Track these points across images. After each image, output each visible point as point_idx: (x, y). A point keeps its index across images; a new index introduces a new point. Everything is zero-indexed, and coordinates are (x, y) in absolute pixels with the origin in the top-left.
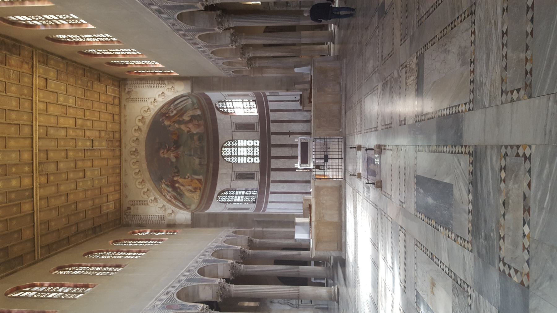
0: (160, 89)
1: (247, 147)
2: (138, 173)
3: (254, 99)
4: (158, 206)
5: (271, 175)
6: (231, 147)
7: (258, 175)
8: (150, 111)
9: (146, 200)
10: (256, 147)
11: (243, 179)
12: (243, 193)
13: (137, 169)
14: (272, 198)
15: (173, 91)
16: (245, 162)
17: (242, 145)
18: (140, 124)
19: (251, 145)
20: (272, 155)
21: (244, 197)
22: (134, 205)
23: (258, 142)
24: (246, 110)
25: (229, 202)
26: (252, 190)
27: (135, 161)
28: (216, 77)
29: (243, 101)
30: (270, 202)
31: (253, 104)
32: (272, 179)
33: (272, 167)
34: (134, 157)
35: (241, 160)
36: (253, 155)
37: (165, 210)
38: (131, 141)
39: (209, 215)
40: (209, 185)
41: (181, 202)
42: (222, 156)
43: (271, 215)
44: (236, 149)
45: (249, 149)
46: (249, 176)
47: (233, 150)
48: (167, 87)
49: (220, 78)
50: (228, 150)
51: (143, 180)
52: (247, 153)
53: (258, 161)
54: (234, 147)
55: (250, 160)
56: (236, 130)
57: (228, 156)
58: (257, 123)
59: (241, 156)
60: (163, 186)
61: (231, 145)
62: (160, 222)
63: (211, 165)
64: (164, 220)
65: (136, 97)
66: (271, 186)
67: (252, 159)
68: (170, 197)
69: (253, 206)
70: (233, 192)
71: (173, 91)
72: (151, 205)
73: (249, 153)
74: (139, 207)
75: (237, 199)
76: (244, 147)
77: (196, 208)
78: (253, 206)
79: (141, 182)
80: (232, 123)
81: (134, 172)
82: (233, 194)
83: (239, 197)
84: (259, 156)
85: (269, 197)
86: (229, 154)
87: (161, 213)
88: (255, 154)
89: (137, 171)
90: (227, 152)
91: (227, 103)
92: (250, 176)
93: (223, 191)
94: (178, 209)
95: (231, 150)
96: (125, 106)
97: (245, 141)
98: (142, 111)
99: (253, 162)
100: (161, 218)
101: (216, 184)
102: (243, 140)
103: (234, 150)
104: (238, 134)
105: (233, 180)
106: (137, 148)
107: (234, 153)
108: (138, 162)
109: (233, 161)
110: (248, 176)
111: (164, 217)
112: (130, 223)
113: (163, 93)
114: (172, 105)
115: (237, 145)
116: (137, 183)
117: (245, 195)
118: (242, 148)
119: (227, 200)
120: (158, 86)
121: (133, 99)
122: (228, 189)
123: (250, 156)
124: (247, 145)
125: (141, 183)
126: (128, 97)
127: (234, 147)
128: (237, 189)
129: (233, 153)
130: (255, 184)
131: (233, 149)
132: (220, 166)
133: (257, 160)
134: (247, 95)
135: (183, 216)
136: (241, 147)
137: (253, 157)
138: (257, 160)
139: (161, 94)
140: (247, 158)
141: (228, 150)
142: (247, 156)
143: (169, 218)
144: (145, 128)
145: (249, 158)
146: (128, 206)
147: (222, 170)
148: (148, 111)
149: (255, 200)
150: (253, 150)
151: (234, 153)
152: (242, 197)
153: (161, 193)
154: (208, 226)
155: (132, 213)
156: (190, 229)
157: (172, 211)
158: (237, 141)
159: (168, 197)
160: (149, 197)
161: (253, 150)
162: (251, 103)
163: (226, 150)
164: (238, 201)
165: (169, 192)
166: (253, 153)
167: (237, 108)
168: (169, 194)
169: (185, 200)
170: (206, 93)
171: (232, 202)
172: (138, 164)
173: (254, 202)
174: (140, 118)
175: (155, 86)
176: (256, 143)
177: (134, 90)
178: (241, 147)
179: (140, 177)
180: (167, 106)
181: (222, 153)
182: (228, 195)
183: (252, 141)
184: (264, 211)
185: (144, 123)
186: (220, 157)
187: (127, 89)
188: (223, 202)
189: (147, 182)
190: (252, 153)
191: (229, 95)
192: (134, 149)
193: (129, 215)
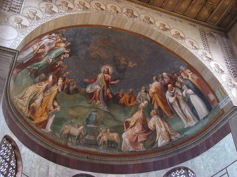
2: (100, 7)
4: (38, 11)
27: (119, 9)
37: (29, 18)
51: (87, 8)
62: (7, 4)
63: (65, 153)
64: (8, 11)
68: (43, 47)
89: (103, 7)
94: (27, 34)
100: (15, 9)
101: (33, 150)
106: (138, 19)
111: (15, 12)
114: (190, 91)
120: (230, 68)
121: (205, 36)
122: (20, 169)
139: (220, 68)
143: (12, 19)
148: (194, 47)
153: (56, 31)
157: (26, 26)
160: (58, 6)
168: (47, 48)
172: (113, 11)
177: (217, 41)
179: (93, 7)
187: (215, 35)
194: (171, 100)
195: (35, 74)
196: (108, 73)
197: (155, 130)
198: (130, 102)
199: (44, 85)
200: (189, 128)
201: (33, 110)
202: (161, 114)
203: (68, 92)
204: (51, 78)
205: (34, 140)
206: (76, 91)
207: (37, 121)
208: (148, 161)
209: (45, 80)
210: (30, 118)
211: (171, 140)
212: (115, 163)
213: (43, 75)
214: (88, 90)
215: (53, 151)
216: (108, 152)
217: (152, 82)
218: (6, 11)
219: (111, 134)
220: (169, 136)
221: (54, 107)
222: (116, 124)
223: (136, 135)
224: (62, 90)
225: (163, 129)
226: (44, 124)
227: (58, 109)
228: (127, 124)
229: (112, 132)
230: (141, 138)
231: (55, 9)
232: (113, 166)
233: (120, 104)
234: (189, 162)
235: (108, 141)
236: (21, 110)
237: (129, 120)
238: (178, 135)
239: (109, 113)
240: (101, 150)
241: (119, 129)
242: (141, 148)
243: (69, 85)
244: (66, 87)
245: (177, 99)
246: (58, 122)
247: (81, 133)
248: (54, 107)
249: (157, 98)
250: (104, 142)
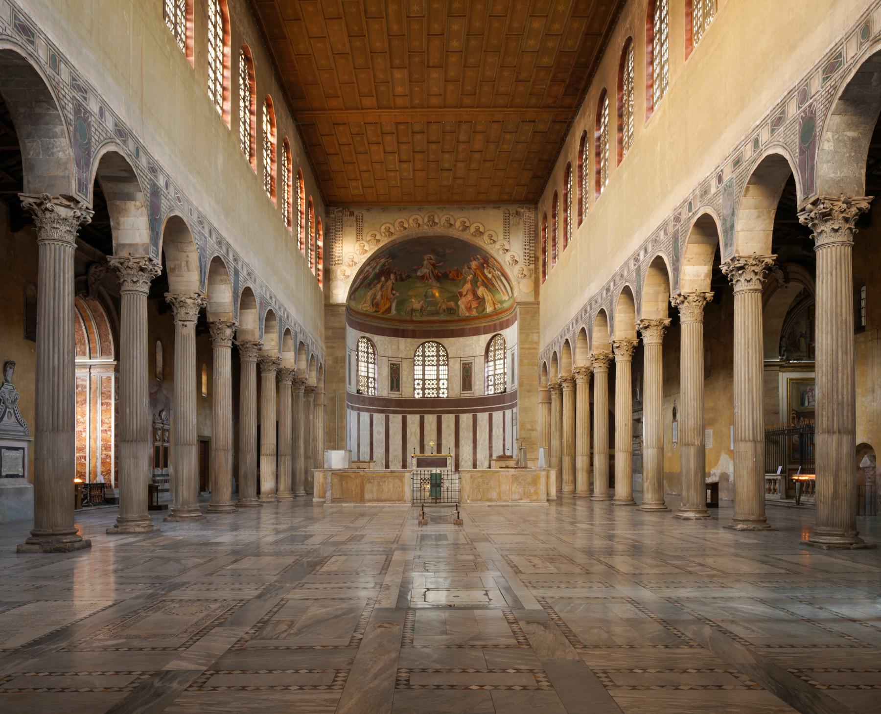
0: (522, 258)
1: (438, 379)
2: (403, 226)
3: (507, 390)
4: (355, 256)
5: (397, 415)
6: (438, 356)
7: (397, 396)
8: (491, 244)
9: (364, 239)
10: (438, 393)
11: (391, 374)
12: (371, 375)
13: (409, 225)
14: (365, 416)
15: (520, 276)
16: (416, 377)
17: (440, 372)
18: (472, 229)
19: (441, 386)
20: (426, 416)
21: (365, 377)
22: (357, 221)
23: (445, 396)
24: (491, 378)
25: (358, 355)
26: (374, 388)
27: (420, 222)
28: (539, 337)
29: (505, 374)
30: (359, 414)
31: (501, 388)
32: (391, 416)
33: (409, 417)
34: (426, 220)
35: (418, 370)
36: (425, 389)
37: (350, 266)
38: (448, 216)
39: (344, 329)
40: (383, 325)
41: (359, 287)
42: (425, 343)
43: (343, 417)
44: (435, 363)
45: (435, 382)
46: (395, 382)
47: (432, 359)
48: (525, 268)
49: (537, 343)
50: (433, 351)
51: (392, 233)
52: (429, 380)
53: (416, 396)
54: (438, 361)
55: (418, 384)
56: (463, 364)
57: (424, 352)
58: (472, 395)
59: (424, 370)
60: (383, 261)
61: (440, 356)
63: (411, 327)
65: (511, 223)
66: (381, 415)
67: (420, 387)
69: (353, 391)
70: (372, 361)
71: (520, 276)
72: (357, 245)
73: (429, 382)
74: (355, 227)
75: (362, 366)
76: (438, 375)
77: (351, 309)
78: (353, 391)
79: (389, 231)
80: (473, 358)
81: (403, 220)
82: (370, 360)
83: (365, 369)
84: (424, 397)
85: (365, 413)
86: (427, 354)
87: (346, 260)
88: (427, 391)
89: (406, 225)
90: (431, 350)
91: (501, 352)
92: (395, 384)
93: (373, 346)
95: (433, 356)
96: (499, 208)
97: (446, 377)
98: (491, 232)
99: (415, 389)
102: (448, 375)
103: (433, 361)
104: (457, 366)
105: (390, 359)
107: (429, 361)
108: (419, 225)
109: (416, 358)
110: (395, 380)
112: (332, 216)
113: (517, 262)
115: (440, 365)
116: (388, 225)
117: (368, 377)
118: (435, 372)
119: (362, 351)
122: (376, 352)
123: (424, 384)
124: (440, 380)
125: (388, 230)
126: (511, 212)
127: (438, 361)
128: (376, 367)
129: (429, 359)
130: (384, 391)
131: (435, 358)
132: (409, 340)
133: (418, 395)
134: (513, 381)
135: (341, 293)
136: (438, 370)
137: (423, 389)
138: (418, 394)
140: (422, 380)
141: (433, 351)
142: (424, 380)
144: (466, 236)
145: (421, 383)
146: (356, 213)
147: (404, 345)
149: (361, 393)
150: (433, 389)
151: (429, 361)
152: (365, 374)
154: (327, 328)
155: (345, 219)
156: (323, 303)
157: (349, 276)
158: (447, 365)
159: (367, 269)
160: (368, 242)
161: (433, 389)
162: (502, 386)
163: (433, 349)
164: (360, 368)
165: (374, 269)
166: (429, 389)
167: (495, 365)
168: (371, 270)
169: (361, 292)
170: (516, 323)
171: (358, 360)
173: (358, 391)
174: (482, 230)
175: (527, 251)
176: (443, 393)
178: (438, 370)
180: (499, 266)
181: (429, 342)
182: (368, 353)
183: (446, 386)
184: (348, 406)
185: (474, 235)
186: (423, 340)
187: (522, 211)
188: (358, 346)
189: (390, 240)
190: (429, 386)
191: (513, 355)
192: (436, 220)
193: (343, 214)
194: (490, 276)
195: (369, 284)
196: (431, 259)
197: (484, 298)
198: (458, 277)
199: (379, 286)
200: (505, 301)
201: (376, 305)
202: (486, 287)
203: (402, 280)
204: (383, 279)
205: (383, 326)
206: (409, 277)
207: (382, 311)
208: (480, 325)
209: (378, 282)
210: (376, 311)
211: (495, 308)
212: (454, 328)
213: (376, 281)
214: (419, 274)
215: (401, 328)
216: (449, 318)
217: (471, 261)
218: (333, 267)
219: (449, 303)
220: (494, 304)
221: (394, 295)
222: (450, 295)
223: (470, 302)
224: (396, 281)
225: (490, 298)
226: (389, 310)
227: (398, 294)
228: (461, 294)
229: (448, 301)
230: (474, 305)
231: (367, 248)
232: (453, 330)
233: (450, 280)
234: (504, 331)
235: (447, 309)
236: (367, 311)
237: (461, 290)
238: (499, 305)
239: (442, 288)
240: (443, 317)
241: (456, 298)
242: (475, 313)
243: (401, 275)
244: (398, 277)
245: (493, 276)
246: (400, 304)
247: (422, 307)
248: (394, 295)
249: (478, 272)
250: (444, 310)
